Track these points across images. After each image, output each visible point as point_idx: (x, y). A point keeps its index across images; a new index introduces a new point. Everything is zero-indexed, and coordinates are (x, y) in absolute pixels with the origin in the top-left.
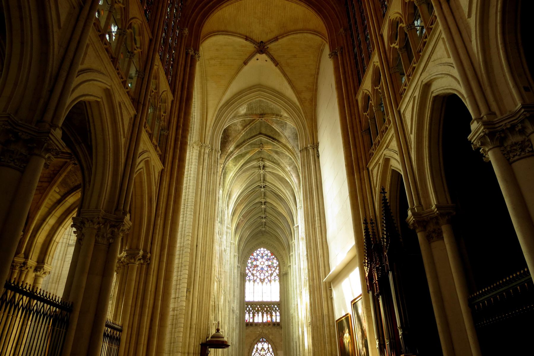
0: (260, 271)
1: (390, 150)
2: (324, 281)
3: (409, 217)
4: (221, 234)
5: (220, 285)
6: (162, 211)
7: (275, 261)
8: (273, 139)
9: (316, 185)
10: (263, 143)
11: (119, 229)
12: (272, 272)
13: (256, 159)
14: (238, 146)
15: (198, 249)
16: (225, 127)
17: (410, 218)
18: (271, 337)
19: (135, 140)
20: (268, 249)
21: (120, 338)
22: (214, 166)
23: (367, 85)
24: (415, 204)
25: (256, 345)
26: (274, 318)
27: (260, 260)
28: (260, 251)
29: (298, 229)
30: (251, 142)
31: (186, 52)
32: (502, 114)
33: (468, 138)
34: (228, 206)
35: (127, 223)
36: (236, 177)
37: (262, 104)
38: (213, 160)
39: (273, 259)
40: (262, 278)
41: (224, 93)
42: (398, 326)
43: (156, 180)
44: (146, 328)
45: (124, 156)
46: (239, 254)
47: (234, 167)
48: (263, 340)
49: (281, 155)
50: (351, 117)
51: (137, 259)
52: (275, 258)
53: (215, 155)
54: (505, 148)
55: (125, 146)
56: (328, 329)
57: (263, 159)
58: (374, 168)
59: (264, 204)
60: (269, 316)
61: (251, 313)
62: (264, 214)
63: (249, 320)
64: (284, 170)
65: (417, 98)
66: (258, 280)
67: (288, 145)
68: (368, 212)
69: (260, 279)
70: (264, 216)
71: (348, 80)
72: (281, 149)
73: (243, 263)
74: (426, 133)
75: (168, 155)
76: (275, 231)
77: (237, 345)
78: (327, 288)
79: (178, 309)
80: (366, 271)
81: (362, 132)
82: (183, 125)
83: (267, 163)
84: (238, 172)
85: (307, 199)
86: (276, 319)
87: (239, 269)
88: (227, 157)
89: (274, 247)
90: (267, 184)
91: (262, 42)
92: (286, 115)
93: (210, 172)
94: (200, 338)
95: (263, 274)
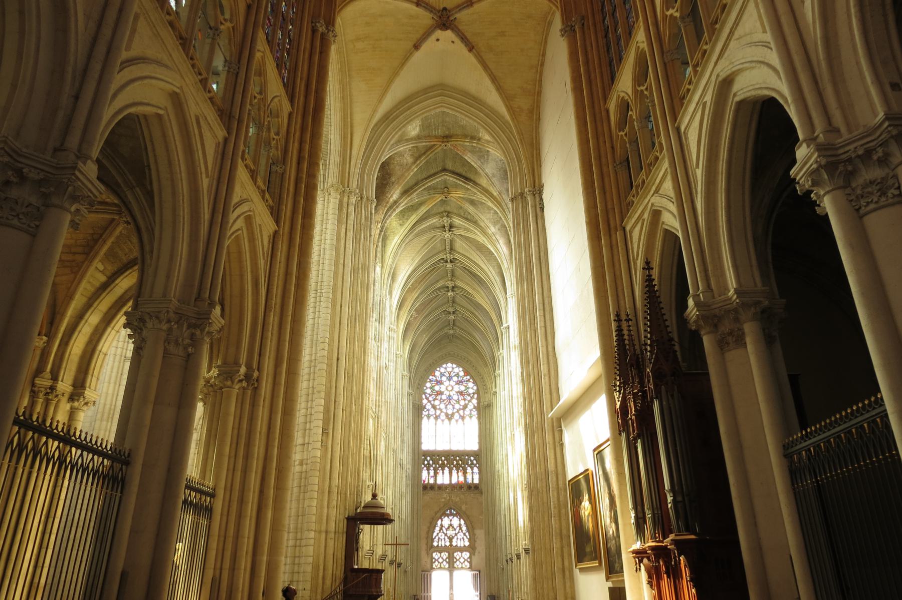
0: (445, 401)
1: (662, 196)
2: (549, 416)
3: (689, 310)
4: (378, 339)
5: (378, 423)
6: (276, 300)
7: (471, 385)
8: (467, 179)
9: (538, 257)
10: (449, 186)
11: (202, 331)
12: (467, 402)
13: (437, 214)
14: (406, 192)
15: (339, 365)
16: (383, 160)
17: (693, 309)
18: (464, 507)
19: (226, 182)
20: (459, 365)
21: (211, 508)
22: (366, 225)
23: (625, 83)
24: (701, 288)
25: (440, 520)
26: (469, 477)
27: (447, 383)
28: (446, 368)
29: (509, 331)
30: (429, 184)
31: (313, 27)
32: (850, 131)
33: (791, 173)
34: (390, 293)
35: (216, 321)
36: (404, 245)
37: (447, 119)
38: (363, 215)
39: (467, 381)
40: (450, 412)
41: (380, 101)
42: (666, 488)
43: (265, 249)
44: (254, 492)
45: (209, 208)
46: (410, 372)
47: (399, 228)
49: (480, 207)
50: (598, 139)
51: (236, 381)
52: (471, 380)
53: (367, 207)
54: (853, 190)
55: (209, 191)
56: (555, 494)
57: (449, 214)
58: (634, 227)
59: (452, 291)
60: (460, 474)
61: (432, 468)
62: (452, 306)
64: (484, 232)
65: (708, 104)
66: (443, 416)
67: (491, 189)
68: (622, 302)
69: (447, 415)
70: (451, 310)
71: (593, 75)
72: (480, 197)
73: (418, 388)
74: (722, 166)
75: (284, 207)
76: (470, 334)
77: (409, 519)
78: (555, 428)
79: (309, 461)
80: (617, 400)
81: (615, 165)
82: (310, 156)
83: (457, 221)
84: (406, 236)
85: (522, 280)
86: (473, 479)
87: (411, 398)
88: (388, 211)
90: (457, 256)
91: (445, 9)
92: (487, 137)
93: (358, 237)
94: (345, 509)
95: (451, 407)
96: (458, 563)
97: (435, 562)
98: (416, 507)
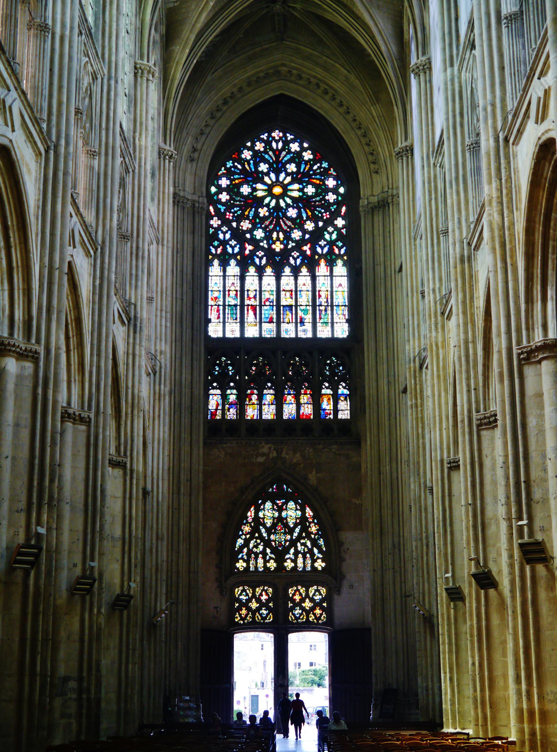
0: (267, 223)
7: (331, 183)
18: (313, 478)
25: (252, 509)
26: (327, 405)
28: (268, 143)
40: (278, 247)
48: (280, 488)
63: (223, 414)
66: (261, 259)
69: (270, 253)
86: (336, 411)
89: (331, 92)
95: (281, 236)
96: (298, 611)
97: (239, 609)
98: (185, 464)
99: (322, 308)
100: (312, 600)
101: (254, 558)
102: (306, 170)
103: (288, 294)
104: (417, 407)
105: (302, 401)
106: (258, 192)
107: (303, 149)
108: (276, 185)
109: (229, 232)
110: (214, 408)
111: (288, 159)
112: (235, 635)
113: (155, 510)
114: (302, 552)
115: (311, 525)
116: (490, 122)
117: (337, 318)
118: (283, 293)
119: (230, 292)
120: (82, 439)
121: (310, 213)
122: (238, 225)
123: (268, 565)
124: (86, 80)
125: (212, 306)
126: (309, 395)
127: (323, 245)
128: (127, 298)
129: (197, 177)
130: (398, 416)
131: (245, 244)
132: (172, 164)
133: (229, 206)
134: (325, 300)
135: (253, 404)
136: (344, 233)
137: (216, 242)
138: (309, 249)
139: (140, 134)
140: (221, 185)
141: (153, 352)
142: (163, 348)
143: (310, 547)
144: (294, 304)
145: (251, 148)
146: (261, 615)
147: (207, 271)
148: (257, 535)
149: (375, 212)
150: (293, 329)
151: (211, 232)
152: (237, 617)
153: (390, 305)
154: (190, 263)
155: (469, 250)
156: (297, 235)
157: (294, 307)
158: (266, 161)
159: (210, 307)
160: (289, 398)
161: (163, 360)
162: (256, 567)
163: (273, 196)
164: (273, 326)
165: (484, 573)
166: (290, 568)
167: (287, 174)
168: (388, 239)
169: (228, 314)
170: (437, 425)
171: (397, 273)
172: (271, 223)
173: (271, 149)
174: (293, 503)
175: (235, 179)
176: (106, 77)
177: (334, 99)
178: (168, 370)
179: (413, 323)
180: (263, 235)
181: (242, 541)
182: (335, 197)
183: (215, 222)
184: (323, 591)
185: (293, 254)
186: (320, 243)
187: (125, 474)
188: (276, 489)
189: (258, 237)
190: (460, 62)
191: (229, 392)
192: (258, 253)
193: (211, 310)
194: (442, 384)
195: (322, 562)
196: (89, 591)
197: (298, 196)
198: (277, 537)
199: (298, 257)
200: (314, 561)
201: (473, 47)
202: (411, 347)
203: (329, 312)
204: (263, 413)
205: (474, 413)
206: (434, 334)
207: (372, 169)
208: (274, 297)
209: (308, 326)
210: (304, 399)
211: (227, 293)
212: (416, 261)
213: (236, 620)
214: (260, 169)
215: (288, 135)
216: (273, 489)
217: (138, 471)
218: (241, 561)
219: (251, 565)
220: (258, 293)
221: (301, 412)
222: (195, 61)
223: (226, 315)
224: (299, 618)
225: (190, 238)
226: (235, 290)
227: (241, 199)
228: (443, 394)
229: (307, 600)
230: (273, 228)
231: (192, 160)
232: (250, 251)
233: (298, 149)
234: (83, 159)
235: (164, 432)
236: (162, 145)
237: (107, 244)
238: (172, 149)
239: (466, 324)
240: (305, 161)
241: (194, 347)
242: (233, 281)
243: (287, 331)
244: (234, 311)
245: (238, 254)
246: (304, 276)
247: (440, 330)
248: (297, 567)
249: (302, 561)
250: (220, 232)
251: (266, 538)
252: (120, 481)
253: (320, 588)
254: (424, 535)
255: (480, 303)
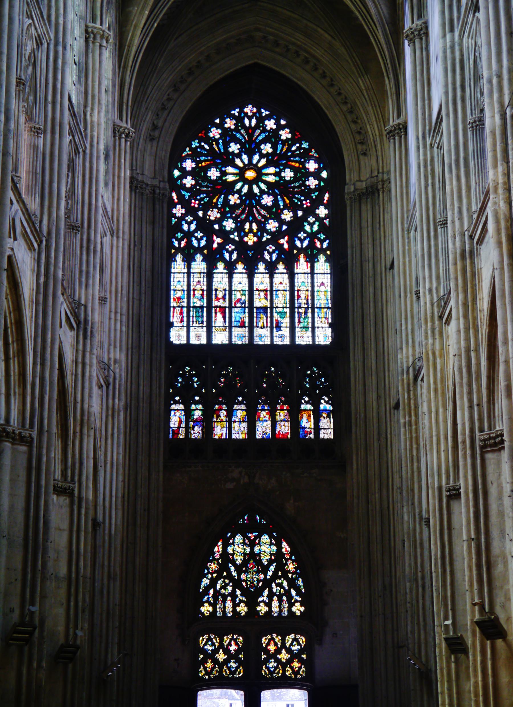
0: (238, 212)
7: (312, 166)
25: (220, 543)
28: (239, 120)
40: (251, 240)
48: (252, 519)
63: (187, 433)
69: (241, 246)
86: (317, 429)
95: (255, 227)
96: (272, 664)
97: (204, 662)
99: (302, 310)
100: (289, 651)
101: (222, 601)
102: (284, 151)
103: (262, 294)
104: (410, 425)
105: (278, 418)
106: (227, 177)
107: (280, 127)
108: (249, 169)
109: (195, 223)
110: (177, 425)
111: (263, 138)
112: (199, 693)
113: (107, 545)
114: (278, 594)
115: (288, 563)
116: (496, 96)
117: (319, 322)
118: (256, 293)
119: (196, 292)
120: (23, 460)
121: (288, 201)
122: (205, 214)
123: (238, 609)
124: (30, 46)
125: (174, 307)
126: (286, 411)
127: (302, 238)
128: (77, 298)
129: (157, 157)
130: (389, 436)
131: (213, 237)
132: (128, 143)
133: (194, 191)
134: (305, 301)
135: (222, 421)
136: (327, 223)
137: (179, 234)
138: (287, 242)
139: (92, 109)
140: (185, 168)
141: (106, 361)
142: (118, 357)
143: (287, 588)
144: (269, 306)
145: (220, 126)
146: (229, 668)
147: (169, 267)
148: (225, 574)
149: (364, 201)
150: (269, 334)
151: (173, 223)
152: (201, 672)
153: (380, 307)
154: (149, 257)
155: (472, 244)
156: (272, 225)
157: (269, 309)
158: (237, 141)
159: (172, 309)
160: (264, 414)
161: (117, 371)
162: (224, 612)
163: (246, 181)
164: (245, 331)
165: (490, 620)
166: (263, 612)
167: (262, 156)
168: (378, 231)
169: (193, 317)
170: (435, 446)
171: (388, 270)
172: (242, 212)
173: (244, 126)
174: (267, 537)
175: (201, 162)
176: (53, 42)
177: (316, 69)
178: (123, 382)
179: (407, 328)
180: (233, 226)
181: (208, 581)
182: (317, 182)
183: (178, 211)
184: (302, 640)
185: (268, 248)
186: (299, 235)
187: (72, 503)
188: (248, 519)
189: (228, 229)
190: (462, 26)
191: (193, 407)
192: (227, 247)
193: (174, 312)
194: (440, 399)
195: (301, 606)
196: (28, 641)
197: (274, 181)
198: (249, 576)
199: (274, 251)
200: (291, 605)
201: (477, 9)
202: (404, 355)
203: (310, 315)
204: (234, 432)
205: (477, 433)
206: (430, 341)
207: (360, 150)
208: (245, 298)
209: (286, 332)
210: (280, 415)
211: (192, 292)
212: (410, 256)
213: (200, 675)
214: (230, 150)
215: (263, 110)
216: (244, 520)
217: (87, 499)
218: (206, 605)
219: (218, 610)
220: (227, 292)
221: (277, 430)
222: (156, 25)
223: (191, 318)
224: (274, 672)
225: (150, 229)
226: (201, 290)
227: (208, 184)
228: (441, 410)
229: (283, 651)
230: (245, 217)
231: (152, 139)
232: (218, 244)
233: (274, 127)
234: (25, 137)
235: (118, 453)
236: (118, 121)
237: (54, 236)
238: (129, 126)
239: (467, 330)
240: (282, 140)
241: (154, 355)
242: (199, 279)
243: (261, 337)
244: (200, 314)
245: (204, 247)
246: (281, 273)
247: (437, 336)
248: (272, 612)
249: (277, 605)
250: (184, 222)
251: (236, 578)
252: (66, 511)
253: (298, 636)
254: (420, 574)
255: (484, 305)
